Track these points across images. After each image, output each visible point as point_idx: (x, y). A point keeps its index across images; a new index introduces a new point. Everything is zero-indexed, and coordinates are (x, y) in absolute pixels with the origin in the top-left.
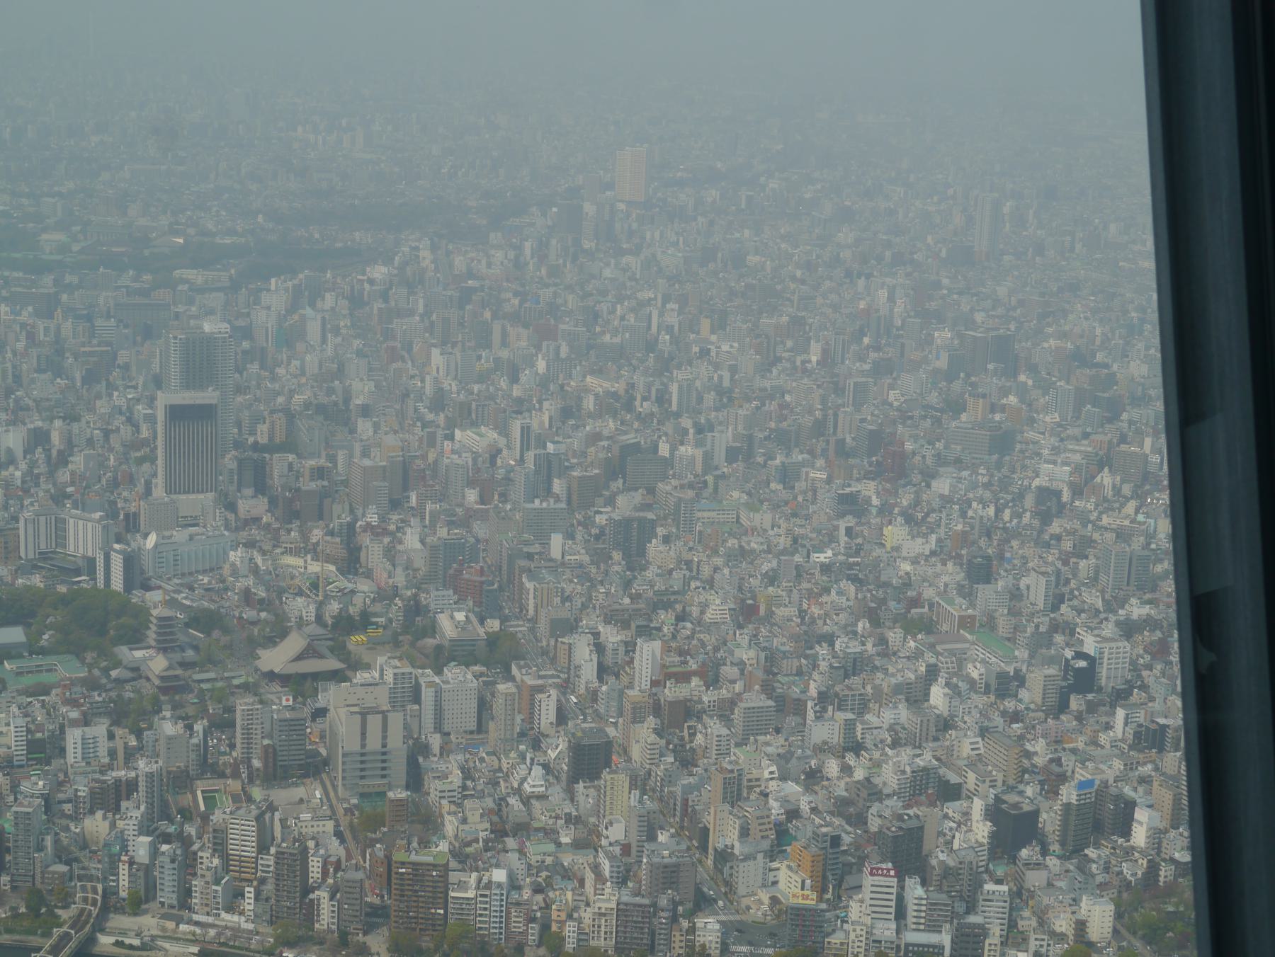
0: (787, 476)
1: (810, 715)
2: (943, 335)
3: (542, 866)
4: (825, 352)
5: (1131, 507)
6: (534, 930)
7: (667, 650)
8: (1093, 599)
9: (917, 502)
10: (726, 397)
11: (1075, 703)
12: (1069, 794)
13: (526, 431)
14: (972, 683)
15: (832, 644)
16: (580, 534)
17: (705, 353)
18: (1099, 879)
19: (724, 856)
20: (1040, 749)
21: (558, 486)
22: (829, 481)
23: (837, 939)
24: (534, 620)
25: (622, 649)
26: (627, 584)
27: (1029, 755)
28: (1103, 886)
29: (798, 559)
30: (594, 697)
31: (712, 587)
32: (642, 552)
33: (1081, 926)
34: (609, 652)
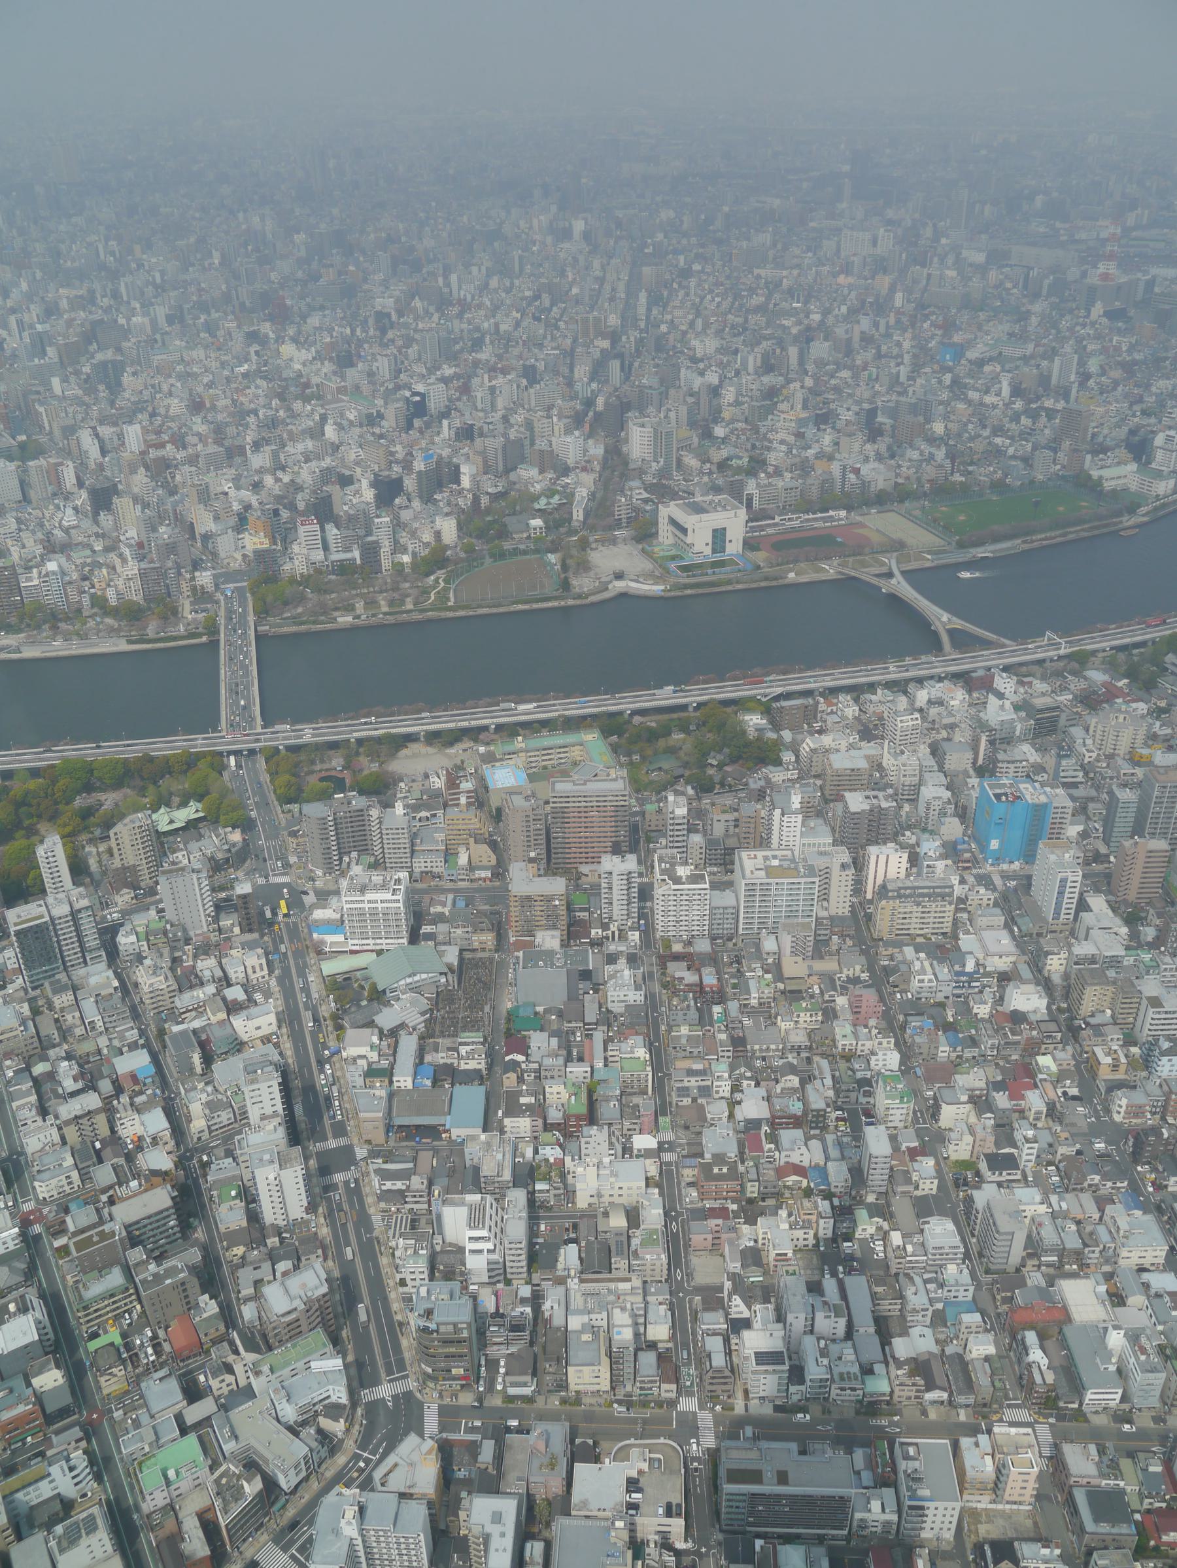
0: (210, 328)
1: (249, 452)
2: (299, 238)
3: (84, 565)
5: (436, 317)
6: (86, 600)
7: (145, 431)
8: (420, 369)
9: (299, 332)
10: (160, 289)
11: (417, 423)
12: (419, 465)
13: (21, 325)
14: (351, 422)
15: (257, 415)
16: (72, 379)
17: (140, 266)
18: (446, 510)
19: (206, 537)
20: (400, 451)
21: (51, 351)
22: (239, 327)
23: (287, 567)
24: (51, 433)
25: (115, 438)
26: (112, 403)
27: (392, 454)
28: (447, 514)
29: (226, 373)
30: (101, 467)
31: (170, 394)
32: (119, 384)
33: (438, 535)
34: (107, 442)
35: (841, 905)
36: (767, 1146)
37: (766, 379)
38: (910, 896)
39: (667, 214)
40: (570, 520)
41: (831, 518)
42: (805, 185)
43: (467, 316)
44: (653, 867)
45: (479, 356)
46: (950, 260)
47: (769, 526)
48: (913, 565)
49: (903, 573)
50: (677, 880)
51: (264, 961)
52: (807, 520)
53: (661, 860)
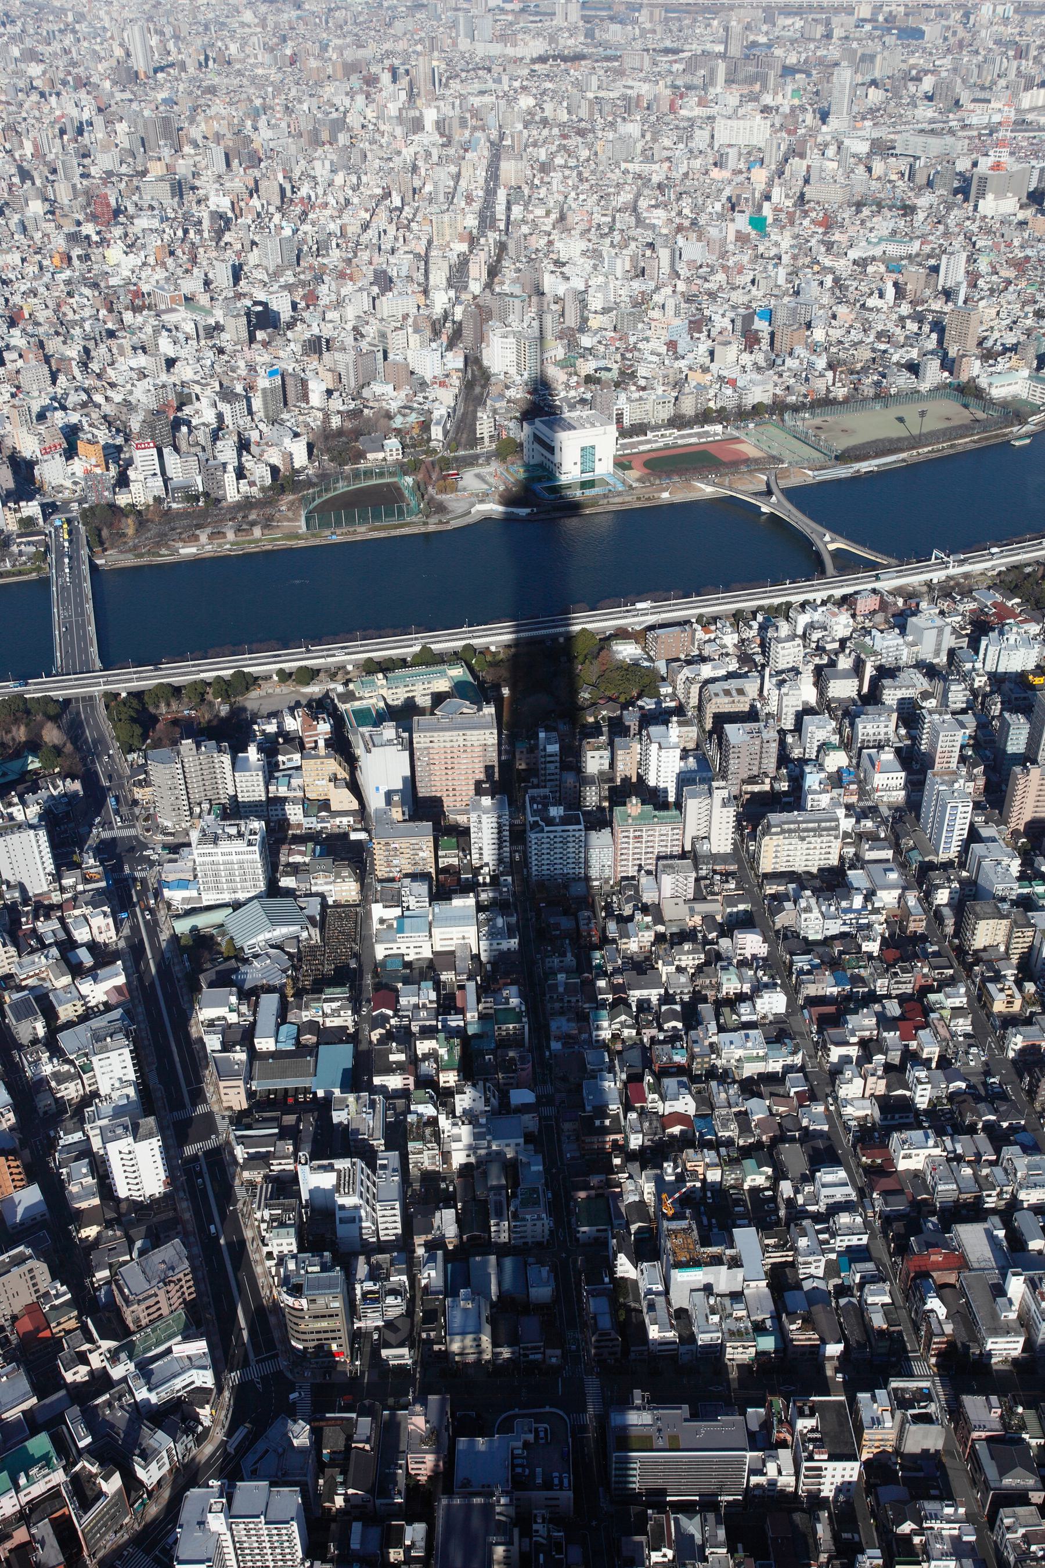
2: (122, 127)
4: (36, 146)
12: (263, 382)
35: (723, 842)
36: (651, 1097)
37: (637, 285)
38: (794, 831)
39: (526, 102)
40: (429, 440)
41: (707, 434)
42: (676, 67)
43: (311, 216)
44: (525, 808)
45: (325, 261)
46: (831, 151)
47: (641, 443)
48: (794, 481)
49: (783, 491)
50: (550, 822)
51: (110, 920)
52: (682, 437)
53: (533, 800)
